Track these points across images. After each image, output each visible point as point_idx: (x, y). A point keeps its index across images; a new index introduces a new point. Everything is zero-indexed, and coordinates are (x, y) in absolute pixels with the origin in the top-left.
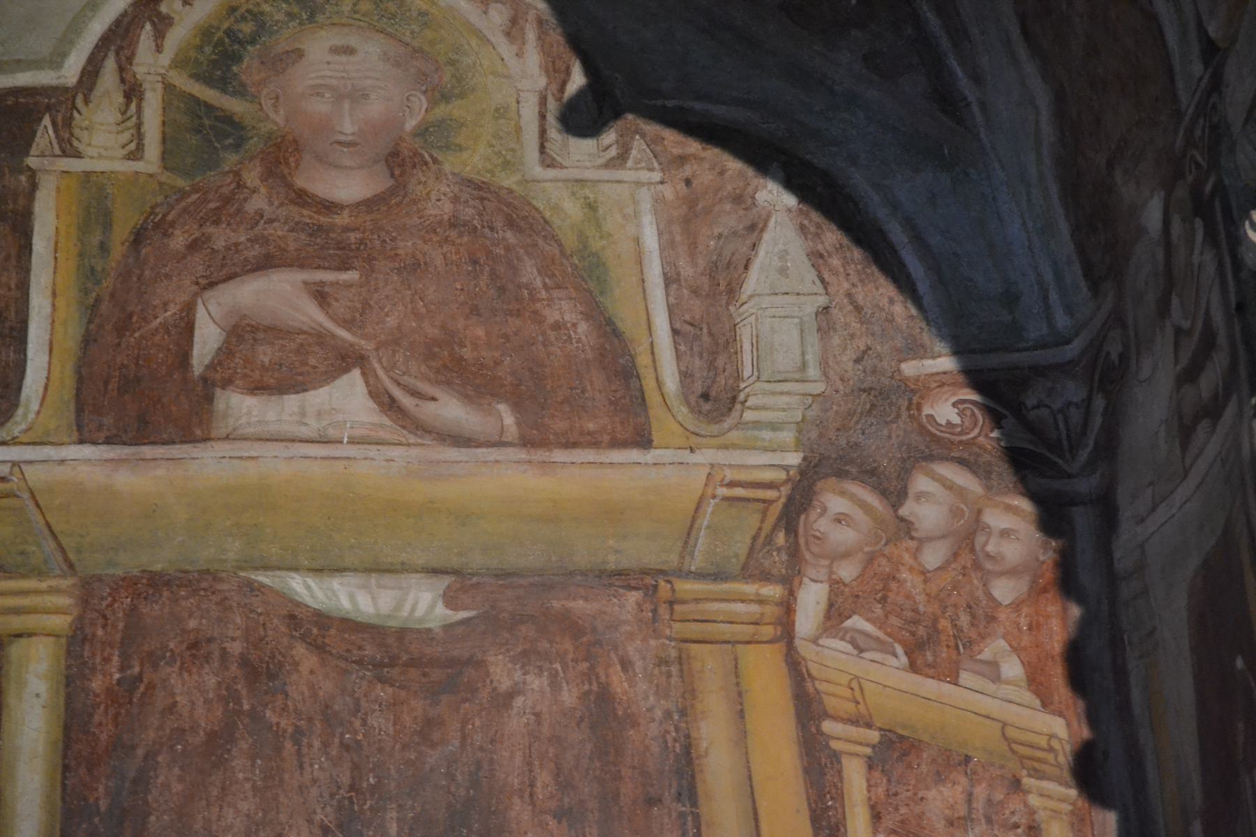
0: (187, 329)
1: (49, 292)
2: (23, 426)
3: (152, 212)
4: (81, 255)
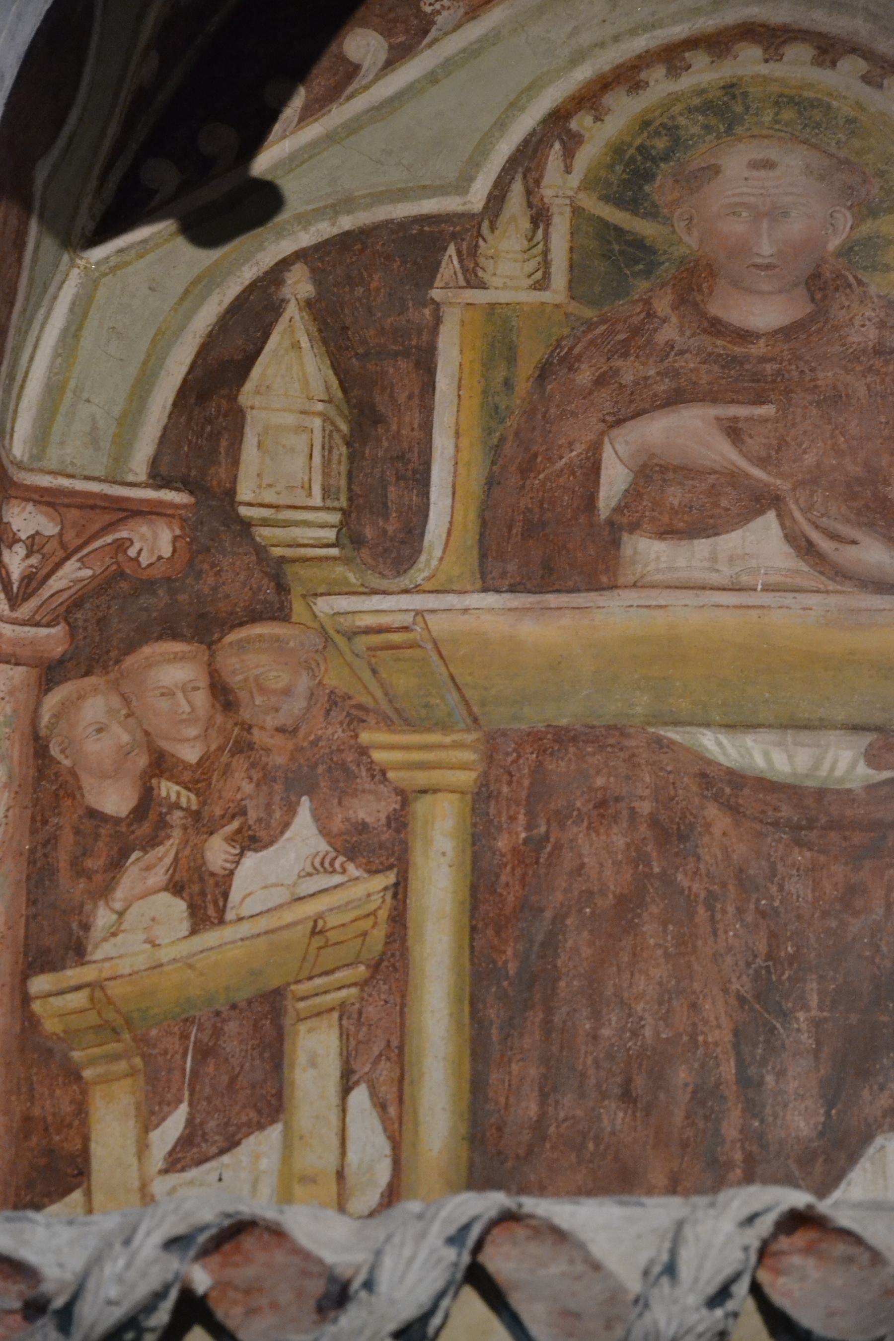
0: (594, 469)
3: (558, 346)
4: (485, 392)
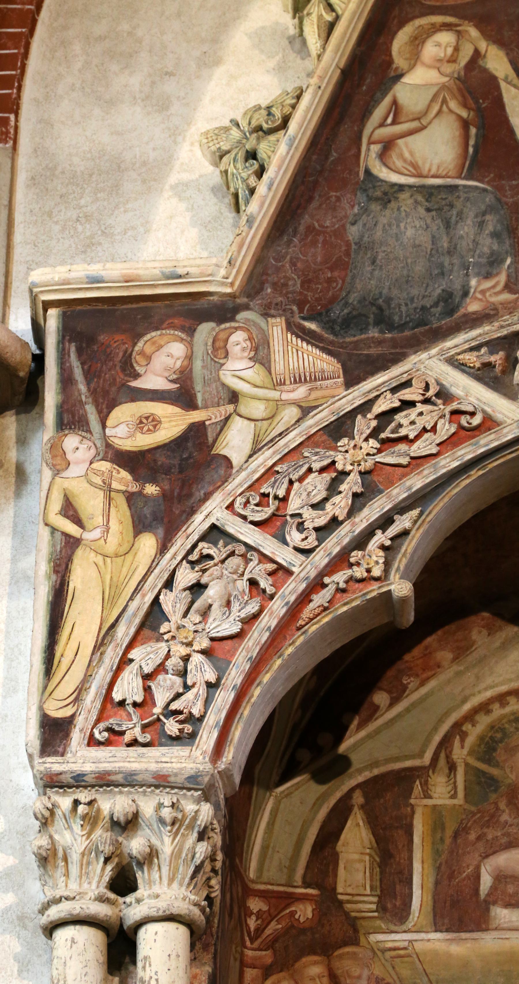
0: (477, 877)
1: (420, 861)
2: (412, 924)
3: (461, 823)
4: (433, 843)
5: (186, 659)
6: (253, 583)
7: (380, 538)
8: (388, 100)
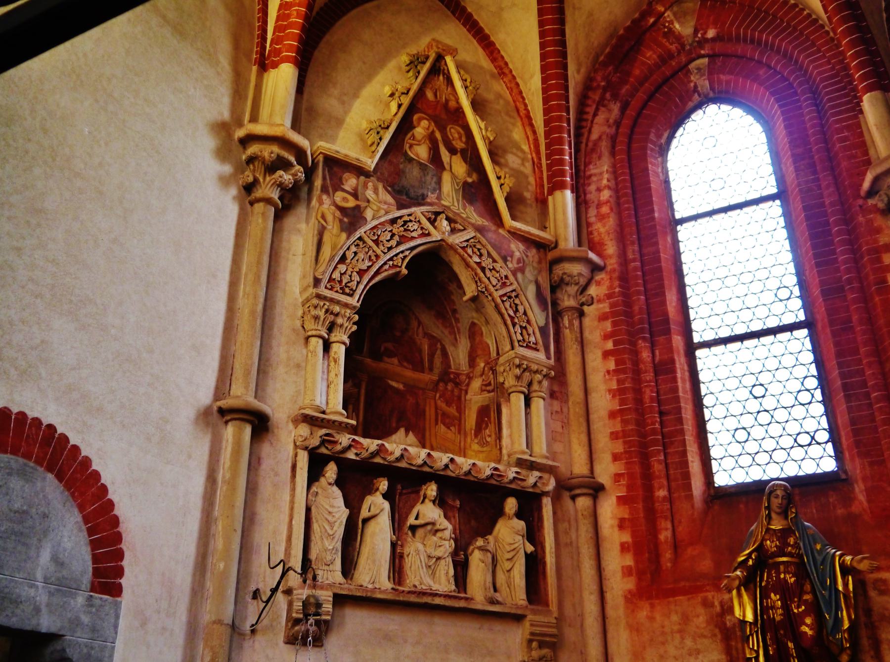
5: (352, 272)
6: (370, 257)
7: (401, 255)
8: (411, 133)
